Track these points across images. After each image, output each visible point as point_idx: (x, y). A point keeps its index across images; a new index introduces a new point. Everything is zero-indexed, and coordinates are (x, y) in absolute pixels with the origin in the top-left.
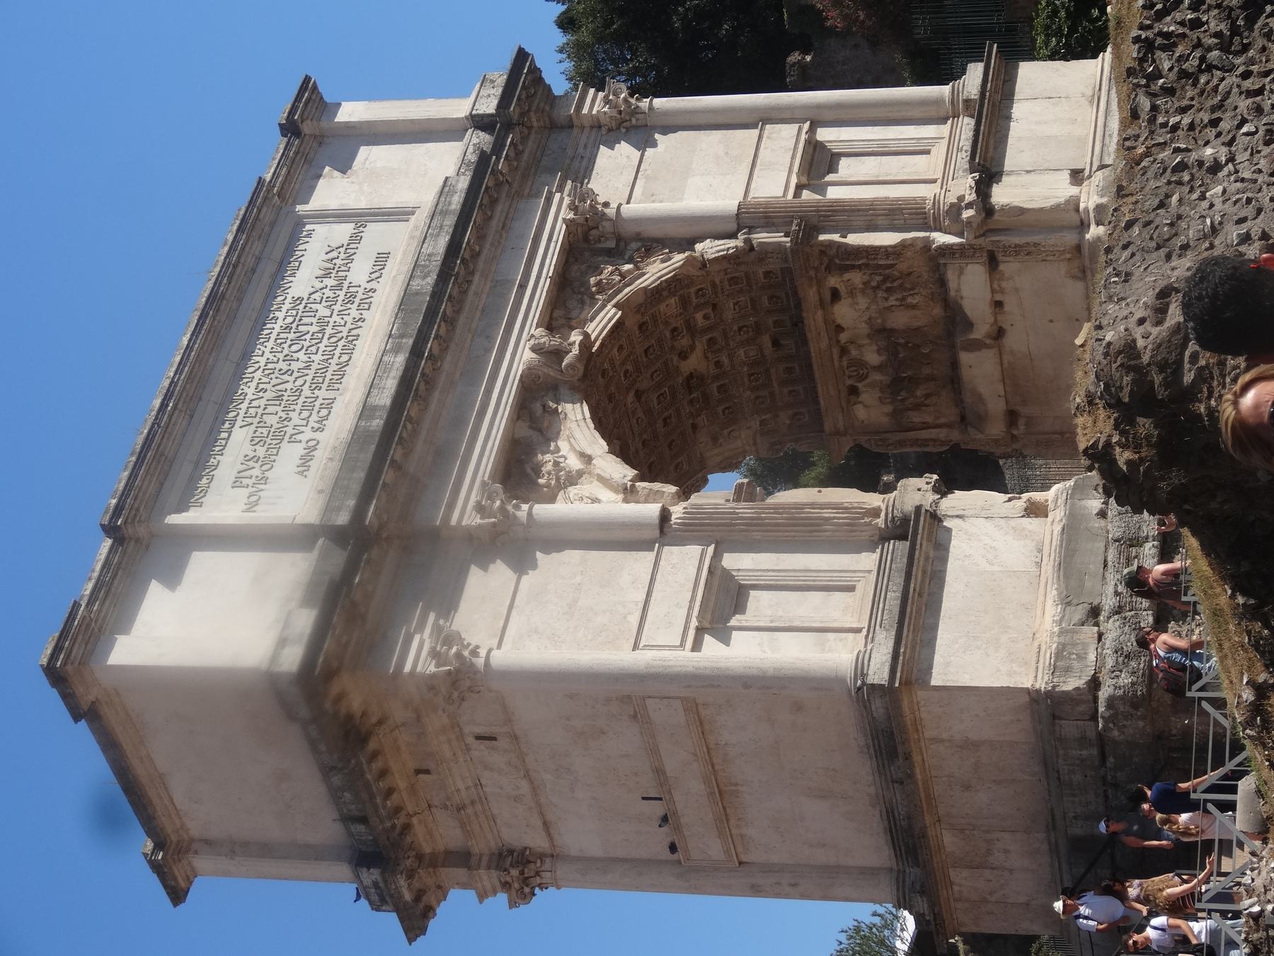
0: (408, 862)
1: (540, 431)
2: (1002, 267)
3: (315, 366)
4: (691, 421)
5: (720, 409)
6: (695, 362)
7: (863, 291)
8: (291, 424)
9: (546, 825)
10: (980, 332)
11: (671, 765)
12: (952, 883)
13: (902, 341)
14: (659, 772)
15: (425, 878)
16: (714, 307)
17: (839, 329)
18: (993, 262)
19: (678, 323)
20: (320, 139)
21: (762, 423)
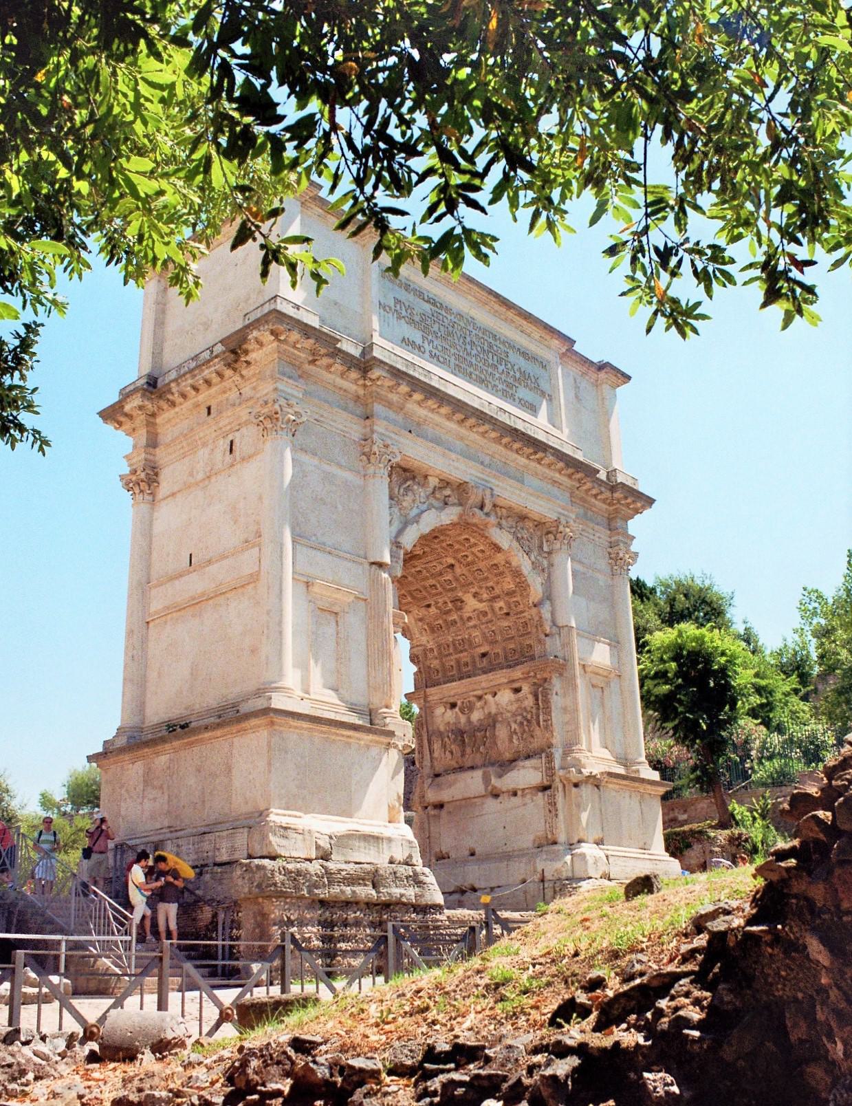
0: (150, 406)
1: (433, 493)
2: (540, 794)
3: (469, 358)
4: (433, 603)
5: (440, 622)
6: (471, 604)
7: (520, 707)
8: (434, 339)
9: (173, 494)
10: (494, 781)
11: (213, 569)
12: (133, 763)
13: (488, 734)
14: (210, 562)
15: (141, 418)
16: (508, 614)
17: (495, 694)
18: (545, 788)
19: (497, 591)
20: (596, 384)
21: (432, 650)
